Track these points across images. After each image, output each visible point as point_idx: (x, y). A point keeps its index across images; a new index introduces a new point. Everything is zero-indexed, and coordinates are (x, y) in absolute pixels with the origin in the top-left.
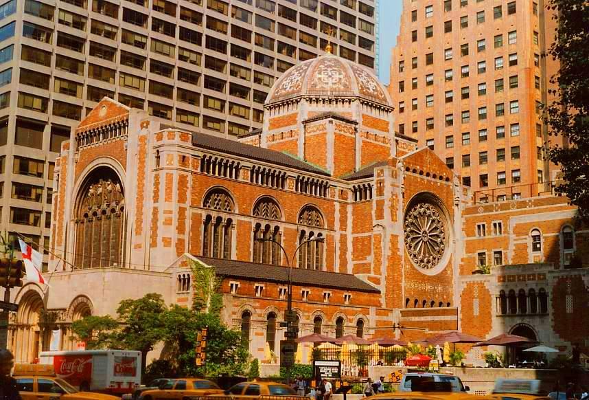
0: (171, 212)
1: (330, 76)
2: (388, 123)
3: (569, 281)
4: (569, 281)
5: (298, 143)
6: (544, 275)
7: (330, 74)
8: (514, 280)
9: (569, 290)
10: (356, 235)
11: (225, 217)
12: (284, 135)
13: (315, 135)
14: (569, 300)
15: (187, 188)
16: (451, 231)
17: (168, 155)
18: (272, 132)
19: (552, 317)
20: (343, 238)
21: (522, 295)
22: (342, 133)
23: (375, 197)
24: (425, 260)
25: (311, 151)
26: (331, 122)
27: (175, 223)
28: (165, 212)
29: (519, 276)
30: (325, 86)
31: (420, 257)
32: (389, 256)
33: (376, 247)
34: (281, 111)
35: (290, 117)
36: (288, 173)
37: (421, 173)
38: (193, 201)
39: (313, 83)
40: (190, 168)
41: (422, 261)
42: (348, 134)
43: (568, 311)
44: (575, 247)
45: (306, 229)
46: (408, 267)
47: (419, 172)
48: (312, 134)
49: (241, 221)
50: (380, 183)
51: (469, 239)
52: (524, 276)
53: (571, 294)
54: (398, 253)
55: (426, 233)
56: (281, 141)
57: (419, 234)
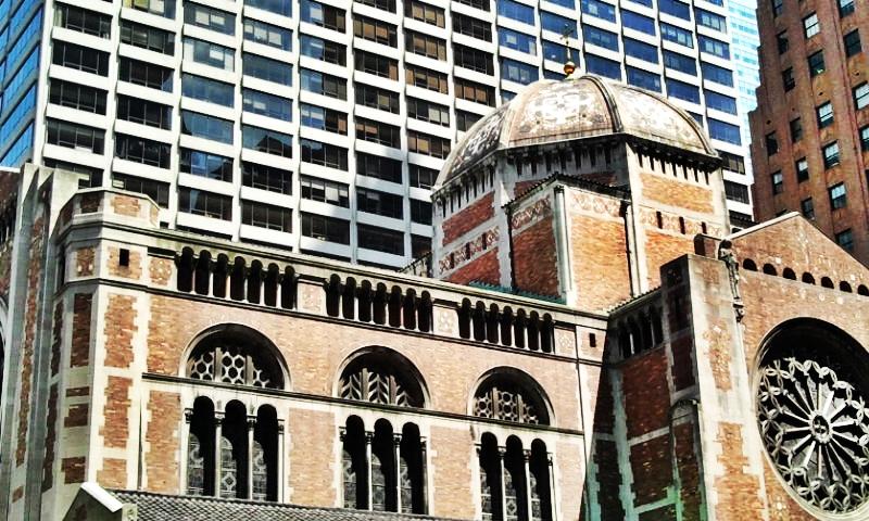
1: (563, 106)
2: (708, 195)
5: (499, 255)
7: (561, 102)
10: (636, 441)
11: (253, 402)
12: (472, 247)
13: (529, 230)
18: (452, 248)
22: (591, 213)
24: (831, 489)
25: (525, 266)
28: (70, 393)
30: (548, 126)
31: (814, 484)
32: (717, 479)
33: (685, 461)
35: (480, 204)
36: (435, 294)
37: (789, 274)
38: (154, 361)
39: (522, 124)
40: (146, 281)
41: (821, 493)
45: (495, 430)
46: (780, 506)
47: (780, 270)
48: (525, 227)
54: (746, 470)
55: (823, 422)
56: (467, 262)
57: (807, 425)
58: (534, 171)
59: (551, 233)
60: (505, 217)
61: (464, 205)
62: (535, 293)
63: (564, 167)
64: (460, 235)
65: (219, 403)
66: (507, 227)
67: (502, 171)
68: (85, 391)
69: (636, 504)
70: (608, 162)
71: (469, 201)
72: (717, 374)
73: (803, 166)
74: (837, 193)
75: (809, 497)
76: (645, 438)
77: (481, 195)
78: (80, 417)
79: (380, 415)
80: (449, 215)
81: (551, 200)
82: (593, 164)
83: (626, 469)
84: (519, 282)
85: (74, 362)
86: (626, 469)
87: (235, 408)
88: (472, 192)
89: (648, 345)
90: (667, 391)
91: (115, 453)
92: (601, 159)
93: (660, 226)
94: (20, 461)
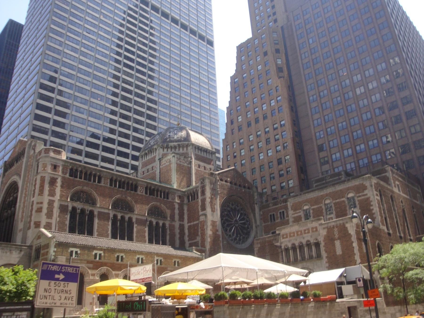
0: (42, 203)
3: (336, 229)
4: (336, 229)
5: (156, 173)
6: (316, 228)
7: (176, 133)
8: (294, 236)
9: (337, 236)
10: (189, 224)
12: (149, 170)
14: (338, 243)
15: (57, 187)
16: (253, 220)
17: (43, 164)
18: (143, 170)
19: (326, 260)
20: (182, 227)
21: (301, 247)
22: (182, 163)
23: (200, 197)
24: (238, 238)
26: (174, 156)
27: (45, 211)
28: (38, 203)
29: (297, 232)
30: (172, 139)
32: (210, 235)
33: (202, 230)
34: (148, 156)
35: (152, 158)
41: (235, 239)
42: (186, 164)
43: (338, 253)
44: (334, 212)
46: (225, 242)
48: (164, 165)
49: (102, 212)
50: (203, 188)
51: (267, 224)
52: (301, 231)
53: (339, 238)
58: (167, 150)
59: (171, 168)
60: (159, 162)
61: (148, 158)
62: (166, 183)
63: (175, 150)
64: (146, 166)
65: (79, 208)
66: (159, 165)
67: (159, 150)
68: (42, 203)
69: (189, 241)
70: (187, 150)
71: (149, 157)
72: (212, 208)
73: (235, 154)
74: (243, 162)
75: (232, 240)
76: (192, 224)
77: (152, 156)
78: (39, 210)
79: (122, 214)
80: (143, 160)
81: (172, 159)
82: (183, 150)
83: (186, 231)
84: (161, 180)
85: (39, 195)
86: (186, 231)
87: (83, 211)
88: (150, 155)
89: (194, 199)
90: (198, 212)
91: (49, 221)
92: (185, 149)
93: (199, 168)
94: (22, 221)
